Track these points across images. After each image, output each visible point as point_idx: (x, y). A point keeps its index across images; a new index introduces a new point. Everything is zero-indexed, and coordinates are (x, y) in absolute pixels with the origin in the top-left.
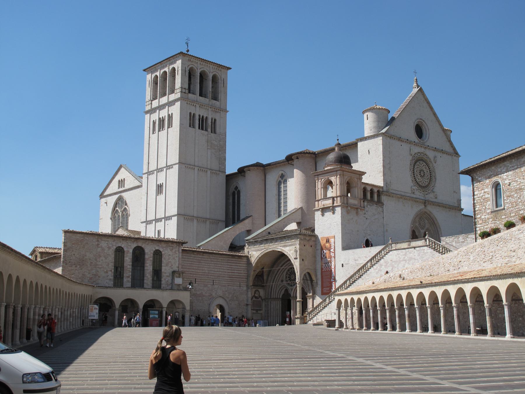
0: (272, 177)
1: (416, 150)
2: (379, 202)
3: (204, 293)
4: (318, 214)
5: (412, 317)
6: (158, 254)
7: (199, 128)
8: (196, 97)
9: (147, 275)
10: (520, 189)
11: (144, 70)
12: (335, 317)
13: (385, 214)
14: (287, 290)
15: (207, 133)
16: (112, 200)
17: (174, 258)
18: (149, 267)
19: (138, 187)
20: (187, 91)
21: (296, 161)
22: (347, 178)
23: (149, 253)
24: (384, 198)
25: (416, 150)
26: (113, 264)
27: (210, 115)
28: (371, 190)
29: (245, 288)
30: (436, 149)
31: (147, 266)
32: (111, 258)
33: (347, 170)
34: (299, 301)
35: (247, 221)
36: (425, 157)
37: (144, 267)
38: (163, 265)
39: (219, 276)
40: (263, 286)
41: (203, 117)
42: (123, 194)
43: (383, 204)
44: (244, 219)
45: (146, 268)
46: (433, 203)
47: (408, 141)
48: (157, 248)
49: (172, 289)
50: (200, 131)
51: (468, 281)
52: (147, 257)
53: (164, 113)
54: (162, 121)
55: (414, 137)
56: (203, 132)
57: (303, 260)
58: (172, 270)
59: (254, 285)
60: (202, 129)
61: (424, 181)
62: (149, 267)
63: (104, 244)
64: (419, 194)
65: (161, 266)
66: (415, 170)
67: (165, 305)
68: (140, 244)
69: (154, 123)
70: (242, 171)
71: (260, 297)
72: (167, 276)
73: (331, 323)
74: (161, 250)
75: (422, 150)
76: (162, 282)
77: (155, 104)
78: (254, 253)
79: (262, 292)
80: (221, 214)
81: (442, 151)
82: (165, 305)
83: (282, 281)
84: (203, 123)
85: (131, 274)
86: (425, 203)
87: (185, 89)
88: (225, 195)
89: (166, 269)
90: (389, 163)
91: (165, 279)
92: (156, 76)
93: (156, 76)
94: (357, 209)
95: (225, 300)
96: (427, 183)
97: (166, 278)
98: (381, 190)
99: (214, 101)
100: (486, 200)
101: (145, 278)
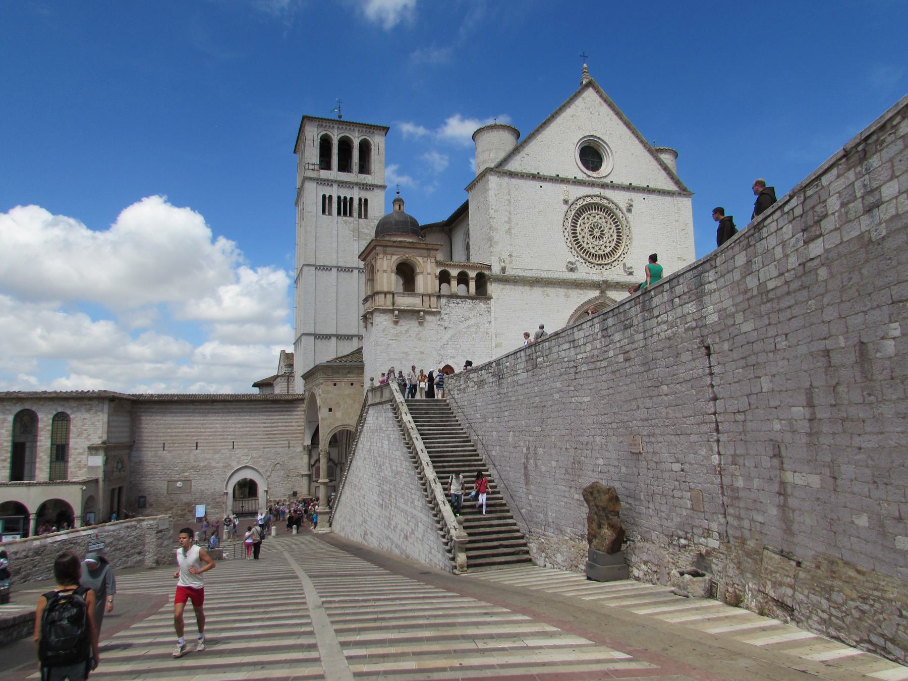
3: (214, 464)
6: (61, 419)
7: (339, 214)
8: (334, 173)
9: (41, 454)
13: (493, 315)
15: (351, 219)
17: (93, 424)
18: (44, 442)
20: (316, 167)
22: (395, 259)
23: (45, 419)
24: (493, 289)
27: (355, 194)
29: (300, 449)
30: (630, 188)
31: (41, 441)
33: (389, 244)
34: (324, 484)
36: (604, 202)
37: (36, 442)
38: (71, 435)
39: (246, 435)
41: (345, 198)
43: (490, 298)
45: (39, 444)
48: (60, 410)
50: (342, 218)
52: (40, 425)
56: (345, 218)
57: (330, 410)
58: (88, 443)
60: (345, 214)
62: (44, 442)
65: (67, 438)
66: (579, 229)
68: (27, 406)
72: (80, 454)
74: (68, 412)
75: (596, 191)
76: (70, 464)
81: (648, 190)
84: (345, 208)
85: (9, 455)
87: (313, 164)
89: (76, 443)
90: (509, 221)
91: (75, 459)
95: (257, 471)
96: (608, 250)
98: (487, 272)
99: (364, 176)
101: (38, 460)
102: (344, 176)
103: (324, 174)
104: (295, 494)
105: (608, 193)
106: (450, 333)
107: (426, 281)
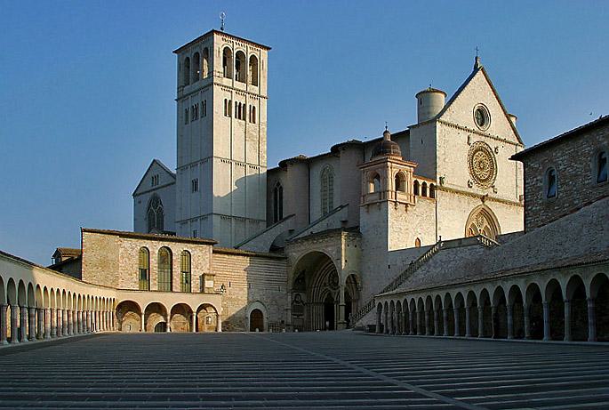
0: (316, 172)
1: (475, 138)
2: (432, 196)
4: (363, 210)
5: (450, 319)
6: (187, 254)
10: (576, 175)
11: (175, 52)
12: (375, 322)
14: (330, 294)
16: (147, 198)
19: (173, 184)
21: (341, 152)
24: (438, 193)
25: (475, 138)
26: (137, 266)
28: (424, 184)
30: (497, 139)
32: (136, 259)
35: (288, 221)
40: (304, 290)
42: (157, 192)
44: (287, 218)
46: (493, 199)
47: (466, 129)
49: (202, 292)
50: (236, 121)
51: (506, 279)
53: (197, 100)
54: (195, 109)
55: (473, 126)
59: (295, 289)
60: (240, 118)
61: (484, 174)
63: (127, 243)
64: (476, 189)
67: (195, 310)
69: (187, 112)
70: (284, 164)
71: (302, 301)
73: (372, 328)
77: (187, 89)
78: (296, 253)
79: (303, 297)
80: (262, 214)
81: (504, 141)
82: (195, 310)
83: (325, 284)
86: (483, 199)
88: (266, 193)
92: (188, 58)
93: (188, 58)
94: (406, 204)
97: (195, 283)
98: (435, 184)
100: (540, 188)
102: (238, 85)
103: (227, 82)
104: (283, 322)
105: (488, 141)
106: (420, 218)
107: (409, 187)
